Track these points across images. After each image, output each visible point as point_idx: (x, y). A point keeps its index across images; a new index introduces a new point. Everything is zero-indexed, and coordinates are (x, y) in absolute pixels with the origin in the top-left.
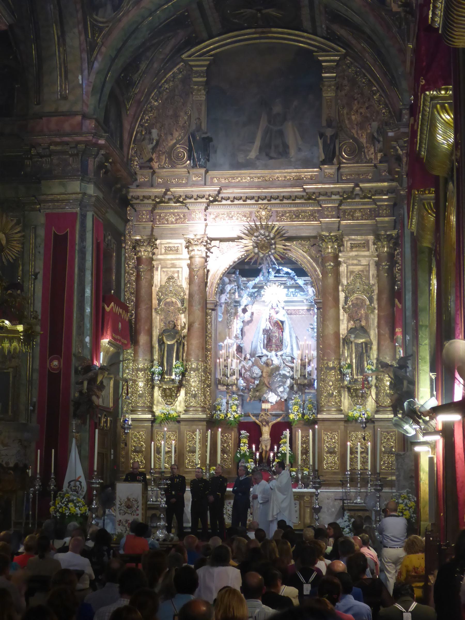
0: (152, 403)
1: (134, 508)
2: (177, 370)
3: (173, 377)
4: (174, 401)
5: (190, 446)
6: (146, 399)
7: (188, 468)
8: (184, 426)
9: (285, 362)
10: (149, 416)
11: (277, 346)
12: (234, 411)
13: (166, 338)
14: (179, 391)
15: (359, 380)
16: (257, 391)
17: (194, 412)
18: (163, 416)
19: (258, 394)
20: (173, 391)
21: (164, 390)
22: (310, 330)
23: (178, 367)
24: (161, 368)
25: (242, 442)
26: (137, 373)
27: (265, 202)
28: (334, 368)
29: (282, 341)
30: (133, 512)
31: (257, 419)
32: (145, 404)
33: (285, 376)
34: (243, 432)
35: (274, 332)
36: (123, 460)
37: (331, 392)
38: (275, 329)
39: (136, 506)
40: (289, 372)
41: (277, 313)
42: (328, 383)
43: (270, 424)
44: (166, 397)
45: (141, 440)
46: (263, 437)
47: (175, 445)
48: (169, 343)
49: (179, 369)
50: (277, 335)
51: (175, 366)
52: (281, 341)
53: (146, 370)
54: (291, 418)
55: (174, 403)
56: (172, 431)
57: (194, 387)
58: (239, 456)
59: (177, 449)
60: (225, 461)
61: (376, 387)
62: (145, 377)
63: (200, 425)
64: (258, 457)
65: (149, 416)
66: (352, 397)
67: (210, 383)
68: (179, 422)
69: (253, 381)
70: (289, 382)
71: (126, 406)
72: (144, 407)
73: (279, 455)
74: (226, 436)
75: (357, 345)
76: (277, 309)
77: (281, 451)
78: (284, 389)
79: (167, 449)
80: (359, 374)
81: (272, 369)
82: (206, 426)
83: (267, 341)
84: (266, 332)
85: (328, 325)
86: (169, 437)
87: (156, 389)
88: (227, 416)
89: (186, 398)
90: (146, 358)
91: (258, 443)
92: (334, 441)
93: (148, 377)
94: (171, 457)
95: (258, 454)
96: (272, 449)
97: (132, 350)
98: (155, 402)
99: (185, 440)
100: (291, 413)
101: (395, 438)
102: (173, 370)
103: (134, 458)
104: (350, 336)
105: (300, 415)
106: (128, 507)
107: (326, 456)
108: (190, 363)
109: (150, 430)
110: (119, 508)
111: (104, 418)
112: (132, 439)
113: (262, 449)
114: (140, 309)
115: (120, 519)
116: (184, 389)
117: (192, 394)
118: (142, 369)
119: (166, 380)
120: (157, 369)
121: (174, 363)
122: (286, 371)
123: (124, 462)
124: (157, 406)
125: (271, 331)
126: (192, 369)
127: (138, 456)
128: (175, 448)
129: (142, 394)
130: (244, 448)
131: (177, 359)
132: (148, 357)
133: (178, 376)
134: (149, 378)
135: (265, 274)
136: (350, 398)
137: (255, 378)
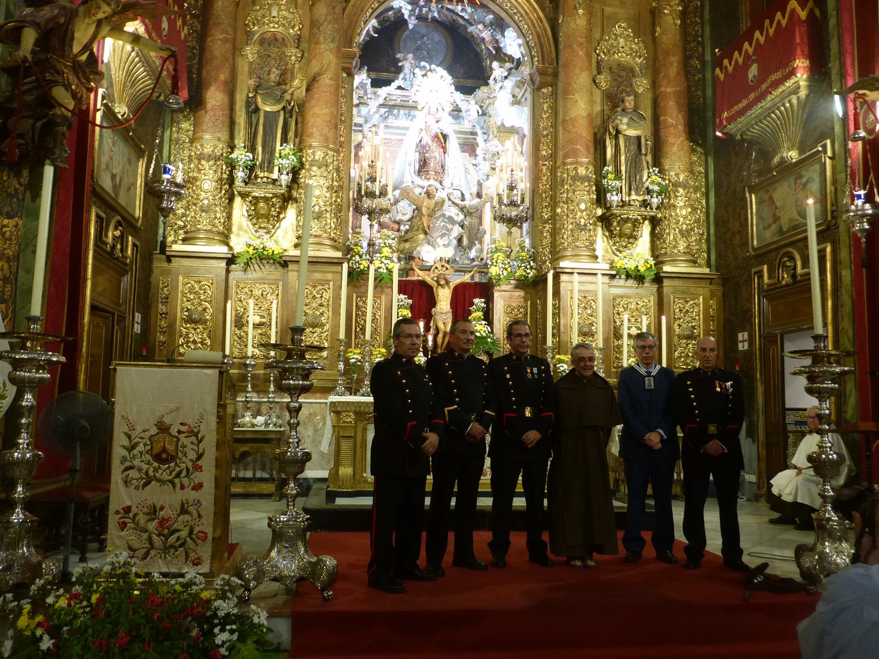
0: (229, 229)
1: (186, 463)
2: (284, 161)
3: (275, 176)
4: (273, 227)
6: (216, 218)
9: (452, 197)
12: (387, 258)
13: (262, 99)
14: (283, 208)
15: (632, 203)
16: (406, 241)
18: (251, 250)
19: (407, 245)
20: (274, 205)
23: (286, 157)
24: (251, 155)
26: (199, 163)
30: (178, 475)
31: (428, 275)
33: (451, 220)
35: (433, 152)
36: (162, 338)
37: (583, 221)
38: (434, 146)
39: (192, 455)
40: (458, 215)
41: (437, 122)
42: (578, 205)
44: (258, 219)
45: (202, 297)
48: (268, 109)
50: (438, 156)
51: (280, 154)
52: (442, 166)
54: (494, 274)
55: (273, 231)
57: (318, 197)
61: (655, 222)
62: (215, 171)
63: (329, 272)
64: (430, 343)
65: (222, 250)
66: (611, 235)
69: (396, 227)
70: (457, 231)
71: (172, 232)
75: (627, 138)
76: (438, 115)
78: (450, 241)
79: (257, 320)
80: (633, 193)
81: (436, 204)
83: (420, 166)
84: (422, 149)
85: (577, 101)
86: (262, 295)
87: (238, 200)
90: (219, 135)
91: (428, 317)
92: (589, 312)
93: (222, 173)
95: (430, 338)
97: (190, 125)
98: (234, 229)
100: (492, 265)
101: (699, 310)
102: (276, 162)
103: (187, 334)
104: (621, 120)
106: (162, 457)
108: (310, 151)
109: (224, 277)
110: (124, 460)
111: (116, 228)
113: (437, 330)
114: (209, 39)
115: (129, 503)
116: (295, 205)
118: (210, 156)
119: (259, 180)
120: (241, 155)
121: (278, 147)
122: (452, 211)
123: (164, 343)
124: (238, 235)
125: (429, 147)
126: (313, 163)
127: (195, 329)
129: (209, 206)
131: (285, 140)
132: (224, 135)
133: (285, 172)
135: (408, 76)
136: (605, 239)
137: (399, 223)
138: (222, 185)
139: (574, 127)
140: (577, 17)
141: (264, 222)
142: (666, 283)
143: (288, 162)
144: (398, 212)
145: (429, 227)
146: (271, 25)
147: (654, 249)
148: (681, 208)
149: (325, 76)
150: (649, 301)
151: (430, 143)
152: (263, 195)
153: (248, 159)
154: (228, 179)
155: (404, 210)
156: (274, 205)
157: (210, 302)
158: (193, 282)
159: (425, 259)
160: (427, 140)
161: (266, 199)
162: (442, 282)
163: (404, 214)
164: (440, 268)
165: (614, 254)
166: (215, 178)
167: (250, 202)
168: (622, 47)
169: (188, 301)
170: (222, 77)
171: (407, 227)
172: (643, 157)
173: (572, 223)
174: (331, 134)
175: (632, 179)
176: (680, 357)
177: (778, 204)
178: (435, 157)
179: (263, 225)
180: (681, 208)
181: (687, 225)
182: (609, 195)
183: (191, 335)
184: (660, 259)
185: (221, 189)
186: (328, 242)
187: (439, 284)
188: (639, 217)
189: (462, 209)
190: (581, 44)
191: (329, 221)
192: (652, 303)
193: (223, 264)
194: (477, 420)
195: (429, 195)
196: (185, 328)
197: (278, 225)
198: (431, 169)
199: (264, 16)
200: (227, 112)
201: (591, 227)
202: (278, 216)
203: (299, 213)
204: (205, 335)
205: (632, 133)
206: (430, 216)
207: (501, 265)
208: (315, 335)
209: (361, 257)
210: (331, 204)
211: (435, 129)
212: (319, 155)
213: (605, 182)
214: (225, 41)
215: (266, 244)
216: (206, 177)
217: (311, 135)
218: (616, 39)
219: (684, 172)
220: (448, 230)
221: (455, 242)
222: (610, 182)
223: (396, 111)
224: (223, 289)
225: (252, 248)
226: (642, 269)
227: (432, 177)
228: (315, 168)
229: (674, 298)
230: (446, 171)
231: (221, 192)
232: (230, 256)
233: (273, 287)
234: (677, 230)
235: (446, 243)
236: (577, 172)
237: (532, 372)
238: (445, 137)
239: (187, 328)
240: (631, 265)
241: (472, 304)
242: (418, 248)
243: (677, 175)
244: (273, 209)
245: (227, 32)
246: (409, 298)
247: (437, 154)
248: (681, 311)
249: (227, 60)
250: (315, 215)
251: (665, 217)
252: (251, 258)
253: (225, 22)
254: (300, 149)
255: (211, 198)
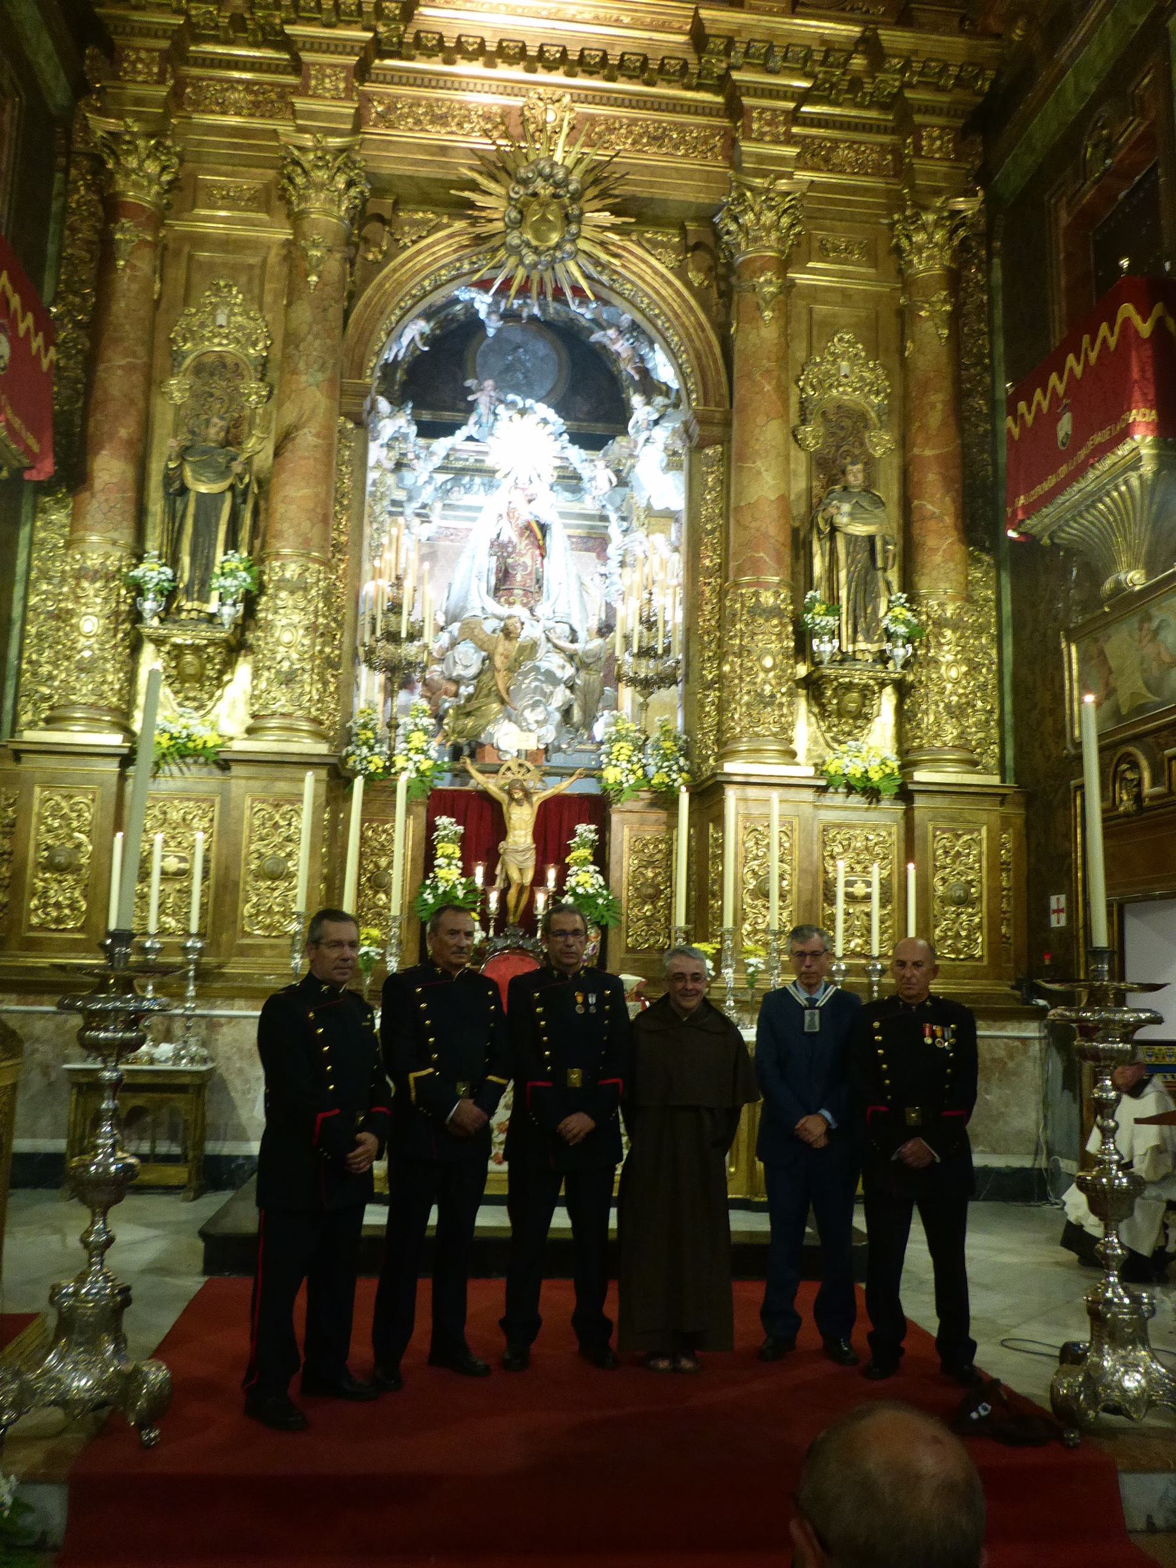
2: (229, 582)
3: (212, 607)
5: (261, 856)
6: (104, 682)
7: (249, 935)
8: (243, 782)
9: (552, 636)
10: (115, 739)
11: (527, 592)
13: (193, 471)
14: (229, 664)
15: (859, 656)
16: (468, 714)
17: (285, 735)
19: (470, 722)
20: (210, 659)
21: (178, 652)
22: (597, 578)
23: (232, 573)
25: (439, 853)
26: (78, 585)
27: (558, 77)
28: (776, 612)
29: (539, 581)
32: (101, 696)
33: (550, 677)
34: (443, 821)
37: (768, 689)
38: (523, 545)
40: (563, 667)
42: (759, 659)
43: (537, 800)
44: (183, 682)
45: (75, 824)
46: (510, 838)
47: (208, 850)
48: (203, 489)
49: (235, 578)
50: (529, 562)
52: (538, 581)
53: (113, 578)
54: (611, 781)
55: (210, 704)
56: (197, 800)
57: (289, 645)
58: (431, 900)
59: (212, 865)
60: (380, 915)
61: (903, 689)
62: (106, 600)
65: (115, 739)
66: (823, 714)
67: (339, 656)
68: (224, 765)
69: (453, 688)
70: (561, 695)
71: (30, 707)
72: (92, 706)
73: (568, 900)
74: (384, 831)
75: (851, 539)
76: (531, 490)
77: (573, 889)
78: (549, 714)
79: (173, 864)
80: (860, 638)
81: (522, 649)
82: (328, 783)
83: (498, 579)
84: (500, 548)
85: (759, 473)
86: (184, 819)
87: (148, 649)
88: (393, 765)
89: (254, 688)
90: (115, 535)
91: (492, 858)
93: (118, 603)
94: (187, 892)
95: (494, 897)
96: (539, 880)
97: (68, 515)
99: (246, 833)
100: (609, 763)
101: (981, 853)
102: (215, 583)
105: (640, 773)
107: (751, 907)
109: (114, 789)
112: (42, 819)
113: (508, 880)
114: (101, 367)
116: (250, 658)
117: (278, 672)
118: (96, 572)
119: (184, 615)
120: (153, 572)
121: (219, 557)
122: (553, 662)
125: (514, 547)
126: (282, 584)
127: (60, 882)
128: (206, 860)
129: (93, 660)
130: (448, 873)
131: (232, 543)
132: (125, 536)
133: (230, 601)
134: (123, 607)
135: (484, 419)
136: (813, 719)
137: (457, 681)
138: (117, 624)
139: (754, 519)
140: (761, 323)
141: (193, 689)
142: (920, 802)
143: (235, 582)
144: (455, 663)
145: (508, 689)
146: (216, 341)
147: (901, 737)
148: (949, 665)
149: (306, 430)
150: (890, 834)
151: (515, 539)
152: (189, 642)
153: (163, 577)
154: (129, 612)
155: (468, 660)
156: (210, 659)
157: (88, 834)
158: (58, 798)
159: (502, 747)
160: (510, 533)
161: (196, 649)
162: (518, 795)
163: (466, 667)
164: (515, 768)
165: (828, 745)
166: (107, 611)
167: (168, 653)
168: (846, 376)
169: (49, 831)
170: (123, 433)
171: (471, 689)
172: (880, 573)
173: (749, 692)
174: (315, 534)
175: (860, 612)
176: (944, 938)
177: (1113, 663)
178: (525, 567)
179: (191, 695)
180: (949, 665)
181: (960, 696)
182: (815, 642)
183: (52, 893)
184: (912, 757)
185: (116, 631)
186: (305, 726)
187: (512, 799)
188: (872, 682)
189: (571, 657)
190: (768, 371)
191: (307, 688)
192: (894, 837)
193: (113, 767)
194: (471, 1095)
195: (508, 633)
196: (42, 880)
197: (218, 693)
198: (517, 585)
199: (202, 325)
200: (130, 494)
201: (784, 700)
202: (219, 678)
203: (256, 674)
204: (77, 894)
205: (860, 530)
206: (511, 670)
207: (624, 765)
208: (276, 894)
209: (371, 748)
210: (312, 658)
211: (526, 514)
212: (292, 571)
213: (808, 618)
214: (130, 369)
215: (192, 730)
216: (90, 610)
217: (279, 536)
218: (834, 362)
219: (953, 599)
220: (544, 694)
221: (557, 716)
222: (819, 619)
223: (466, 479)
224: (112, 808)
225: (167, 736)
226: (875, 776)
227: (518, 600)
228: (283, 594)
229: (935, 829)
230: (545, 589)
231: (115, 636)
232: (125, 751)
233: (204, 806)
234: (942, 705)
235: (541, 717)
236: (758, 600)
237: (585, 1002)
238: (544, 528)
239: (44, 880)
240: (855, 769)
241: (573, 834)
242: (490, 728)
243: (941, 605)
244: (209, 666)
245: (134, 354)
246: (458, 823)
247: (527, 560)
248: (946, 853)
249: (132, 402)
250: (282, 678)
251: (920, 682)
252: (164, 755)
253: (132, 336)
254: (257, 561)
255: (96, 646)
